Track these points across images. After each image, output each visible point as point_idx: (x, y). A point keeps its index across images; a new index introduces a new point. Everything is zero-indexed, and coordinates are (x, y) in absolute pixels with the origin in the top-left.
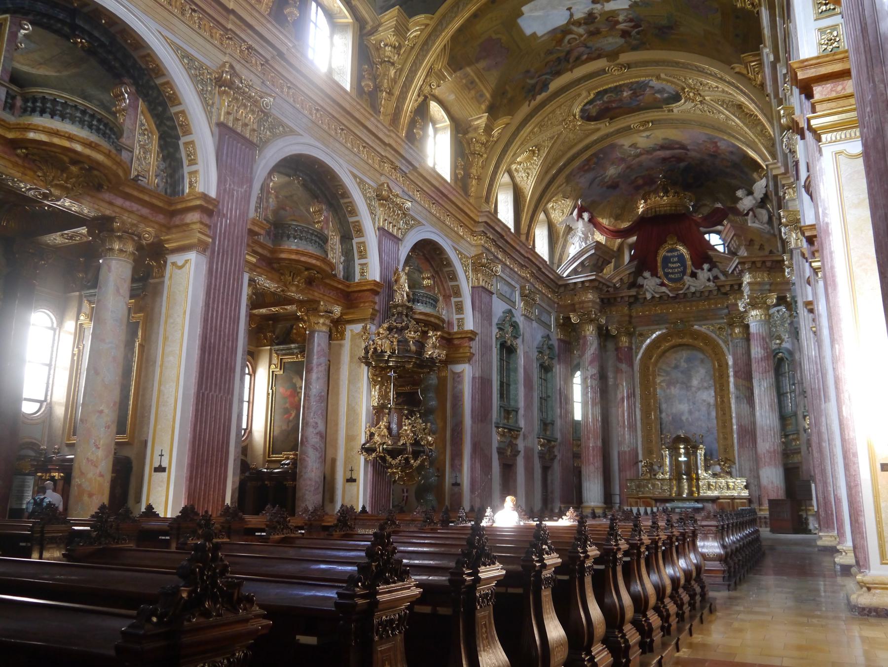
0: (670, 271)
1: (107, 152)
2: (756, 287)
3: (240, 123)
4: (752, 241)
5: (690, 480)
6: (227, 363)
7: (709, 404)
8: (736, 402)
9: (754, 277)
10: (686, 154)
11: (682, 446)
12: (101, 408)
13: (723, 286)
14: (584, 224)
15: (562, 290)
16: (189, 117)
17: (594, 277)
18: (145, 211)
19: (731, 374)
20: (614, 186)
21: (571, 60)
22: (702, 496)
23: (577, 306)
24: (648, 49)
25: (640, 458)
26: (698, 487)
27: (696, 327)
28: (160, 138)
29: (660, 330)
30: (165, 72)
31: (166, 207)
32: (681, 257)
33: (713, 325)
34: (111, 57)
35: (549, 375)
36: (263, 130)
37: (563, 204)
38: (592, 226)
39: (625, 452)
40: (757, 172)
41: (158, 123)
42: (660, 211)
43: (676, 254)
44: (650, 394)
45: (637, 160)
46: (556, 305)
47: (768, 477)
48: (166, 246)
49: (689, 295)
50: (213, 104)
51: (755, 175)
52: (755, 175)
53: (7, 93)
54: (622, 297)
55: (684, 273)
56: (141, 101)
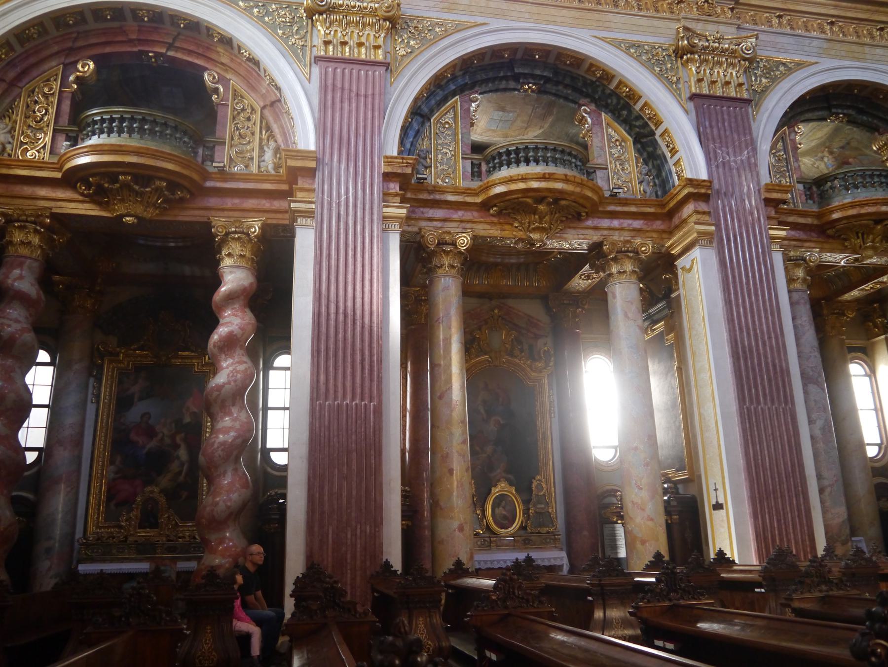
1: (563, 177)
3: (719, 85)
6: (774, 366)
12: (635, 445)
16: (654, 106)
18: (637, 224)
28: (636, 142)
30: (614, 73)
31: (659, 211)
34: (560, 87)
36: (756, 80)
41: (627, 128)
48: (673, 252)
50: (678, 80)
53: (472, 163)
56: (603, 114)
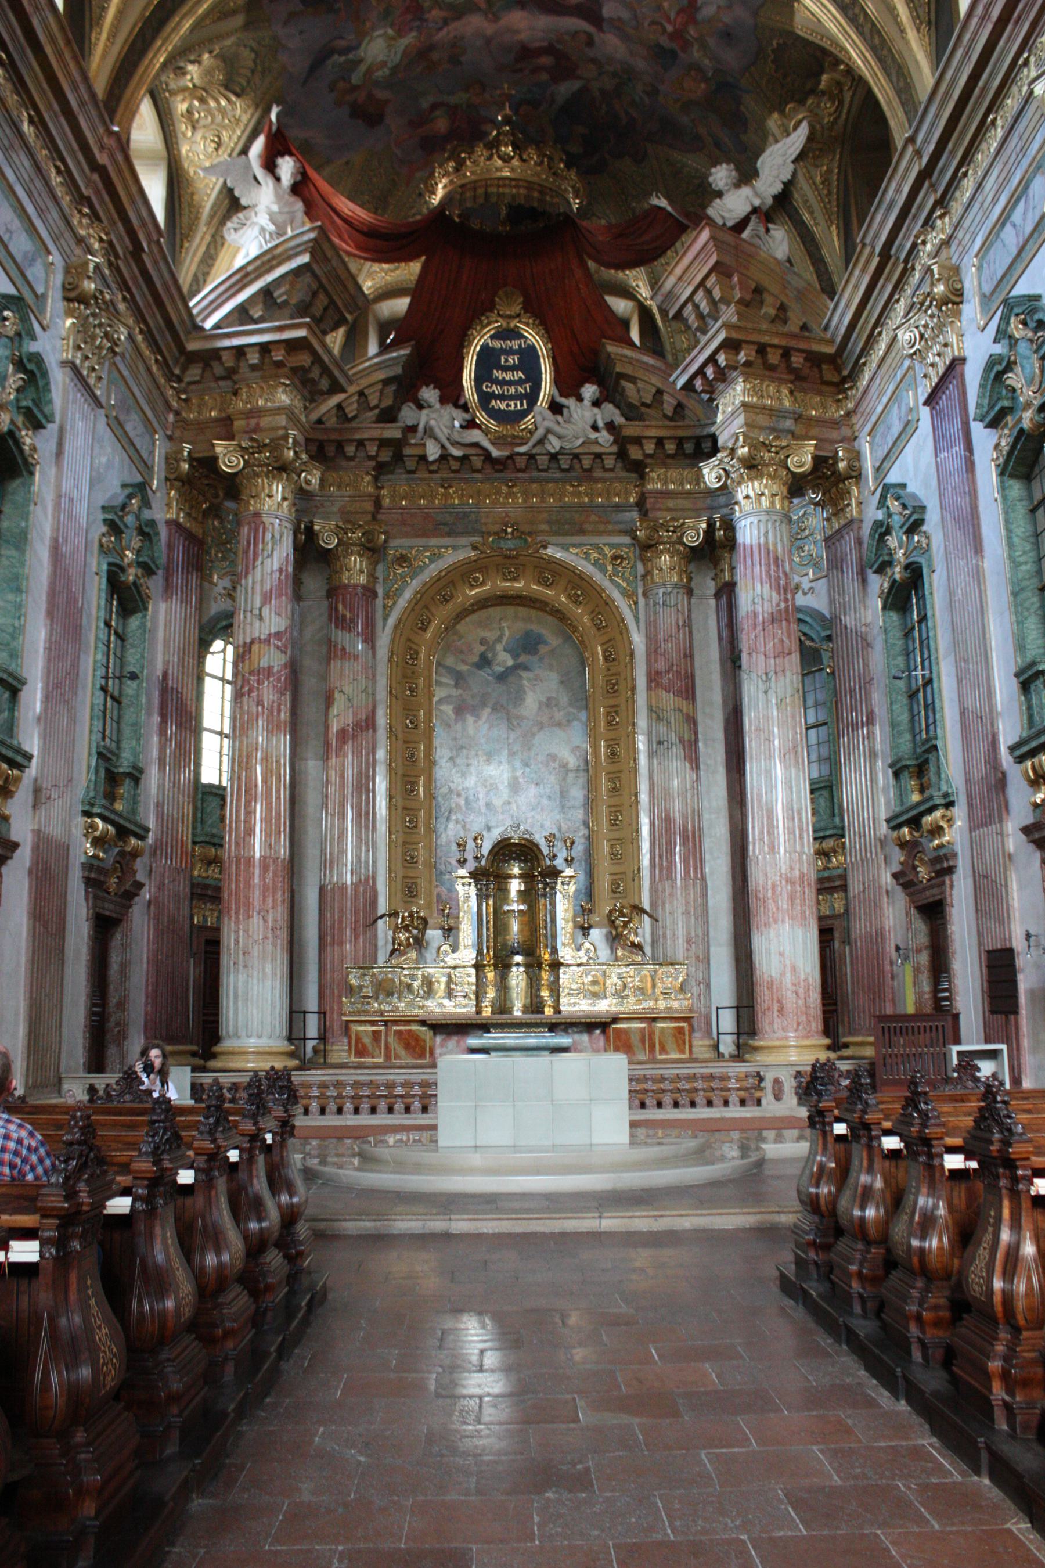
0: (496, 389)
2: (762, 420)
4: (758, 291)
5: (533, 965)
7: (564, 766)
8: (651, 755)
9: (755, 391)
10: (590, 42)
11: (516, 871)
13: (638, 441)
15: (194, 372)
17: (301, 333)
19: (641, 681)
22: (571, 1015)
23: (239, 424)
25: (383, 907)
26: (555, 990)
27: (554, 552)
29: (454, 548)
32: (529, 359)
33: (597, 547)
35: (134, 622)
37: (223, 111)
38: (299, 206)
39: (343, 887)
40: (782, 112)
42: (499, 195)
43: (515, 344)
44: (416, 727)
45: (456, 28)
46: (171, 418)
47: (781, 954)
49: (543, 461)
51: (773, 122)
52: (773, 122)
54: (361, 444)
55: (532, 398)
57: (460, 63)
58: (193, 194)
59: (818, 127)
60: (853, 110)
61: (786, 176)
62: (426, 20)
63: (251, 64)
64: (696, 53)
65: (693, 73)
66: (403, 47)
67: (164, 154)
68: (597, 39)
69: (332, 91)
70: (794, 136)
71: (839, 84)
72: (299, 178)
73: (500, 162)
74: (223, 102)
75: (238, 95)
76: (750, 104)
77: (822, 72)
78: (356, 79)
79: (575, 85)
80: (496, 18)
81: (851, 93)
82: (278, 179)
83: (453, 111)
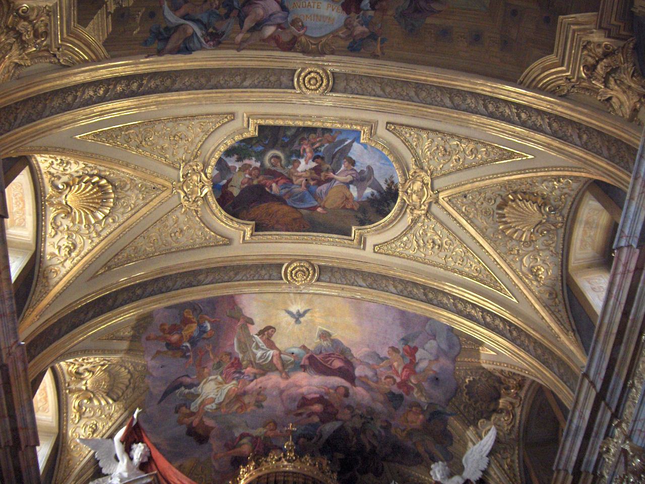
10: (347, 395)
14: (129, 468)
20: (199, 436)
21: (248, 23)
24: (375, 56)
40: (476, 426)
51: (470, 433)
57: (262, 406)
58: (69, 460)
59: (501, 434)
60: (524, 417)
61: (484, 466)
62: (243, 374)
63: (126, 381)
64: (416, 394)
65: (414, 409)
66: (226, 391)
67: (57, 430)
68: (351, 391)
69: (177, 412)
70: (485, 439)
71: (511, 403)
72: (146, 460)
73: (286, 463)
74: (103, 403)
75: (114, 401)
76: (454, 424)
77: (499, 397)
78: (194, 407)
79: (336, 425)
80: (288, 377)
81: (520, 409)
82: (131, 459)
83: (255, 440)
